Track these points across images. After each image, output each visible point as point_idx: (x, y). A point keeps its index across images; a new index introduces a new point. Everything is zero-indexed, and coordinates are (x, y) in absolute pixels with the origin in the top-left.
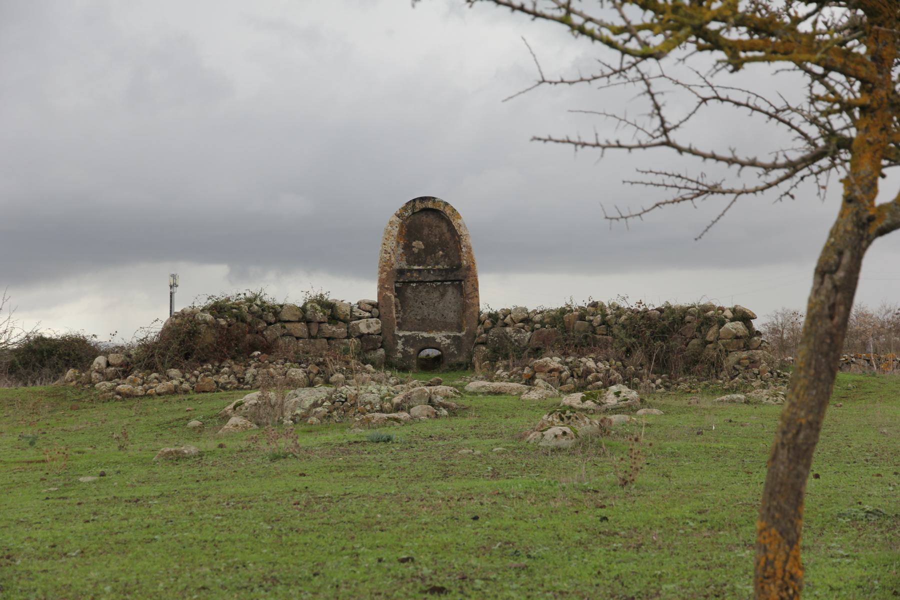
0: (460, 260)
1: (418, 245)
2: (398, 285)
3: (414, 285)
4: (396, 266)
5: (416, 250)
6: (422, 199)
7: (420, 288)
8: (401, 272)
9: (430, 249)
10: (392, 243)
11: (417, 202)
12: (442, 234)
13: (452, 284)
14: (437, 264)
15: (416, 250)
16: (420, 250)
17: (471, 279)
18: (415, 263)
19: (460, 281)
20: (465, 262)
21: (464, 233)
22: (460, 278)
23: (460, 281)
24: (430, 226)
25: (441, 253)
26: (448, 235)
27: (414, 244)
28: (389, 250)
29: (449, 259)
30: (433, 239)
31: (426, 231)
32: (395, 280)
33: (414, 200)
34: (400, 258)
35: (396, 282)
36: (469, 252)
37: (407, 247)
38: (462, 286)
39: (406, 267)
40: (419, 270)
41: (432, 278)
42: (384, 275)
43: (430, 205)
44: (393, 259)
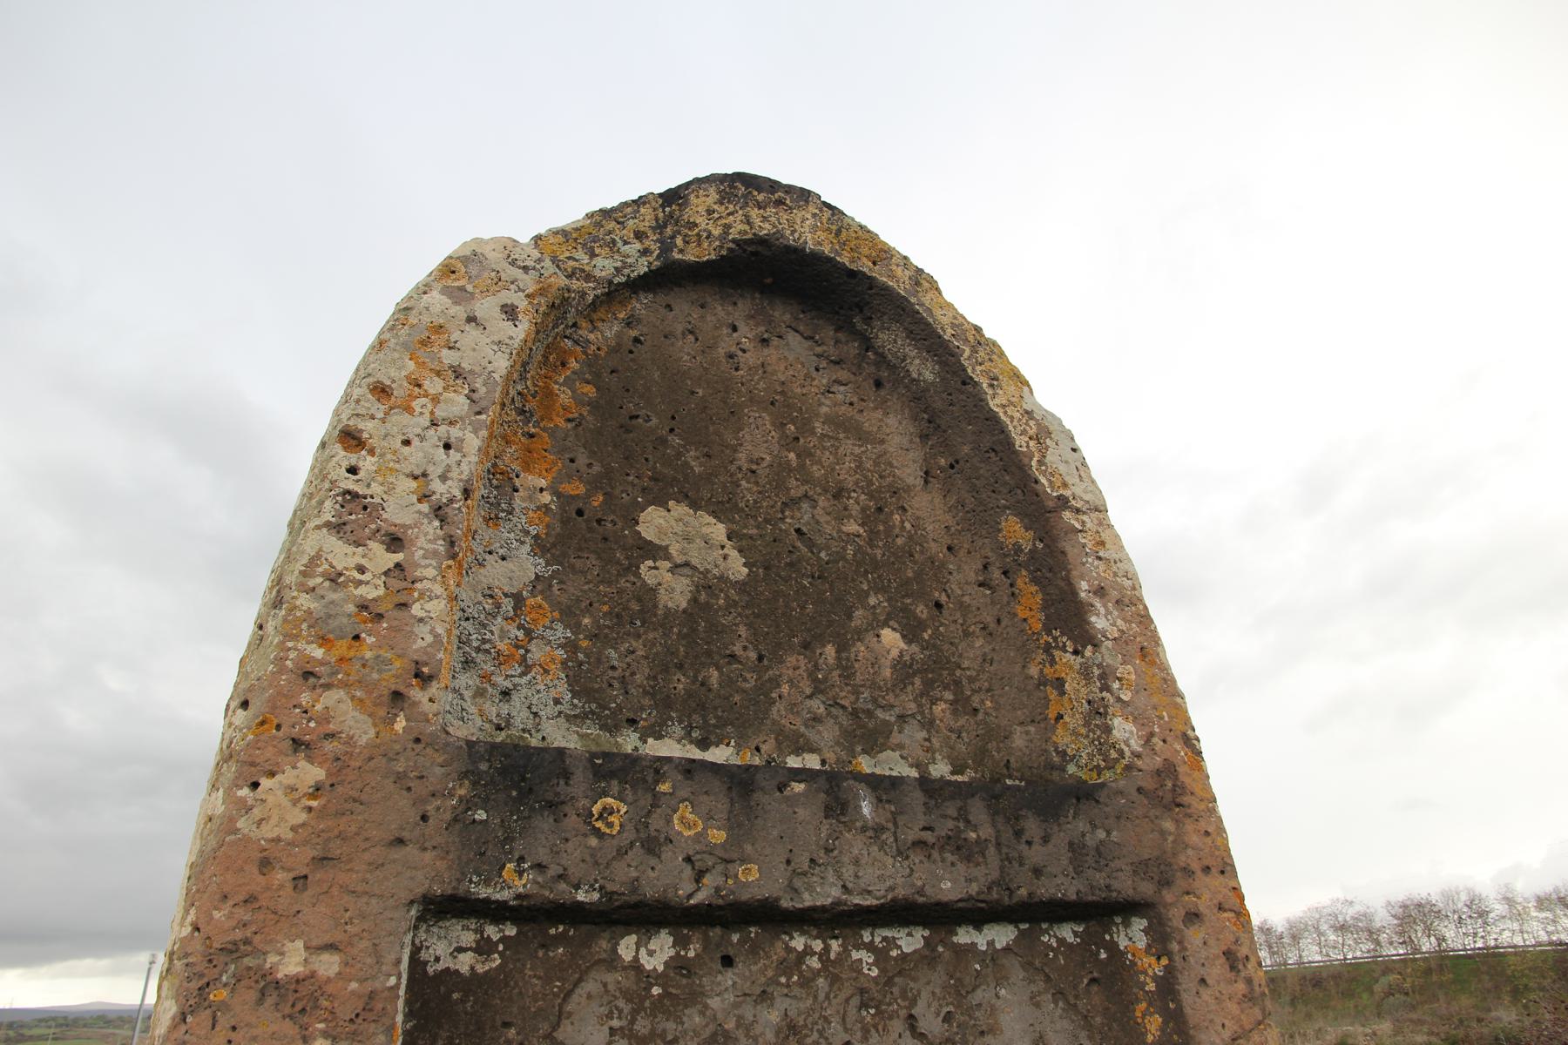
0: (1047, 723)
1: (688, 543)
2: (454, 949)
3: (658, 952)
4: (458, 711)
5: (675, 592)
6: (742, 187)
7: (723, 992)
8: (515, 778)
9: (796, 597)
10: (446, 448)
11: (698, 208)
12: (884, 502)
13: (1025, 946)
14: (875, 741)
15: (675, 592)
16: (707, 585)
17: (1207, 891)
18: (664, 711)
19: (1100, 912)
20: (1123, 730)
21: (1077, 489)
22: (1126, 885)
23: (1100, 912)
24: (787, 411)
25: (891, 638)
26: (929, 512)
27: (654, 523)
28: (401, 508)
29: (961, 705)
30: (815, 515)
31: (758, 441)
32: (427, 870)
33: (674, 197)
34: (503, 634)
35: (441, 908)
36: (1144, 645)
37: (590, 541)
38: (1115, 975)
39: (561, 736)
40: (740, 782)
41: (877, 876)
42: (282, 806)
43: (807, 234)
44: (432, 610)
